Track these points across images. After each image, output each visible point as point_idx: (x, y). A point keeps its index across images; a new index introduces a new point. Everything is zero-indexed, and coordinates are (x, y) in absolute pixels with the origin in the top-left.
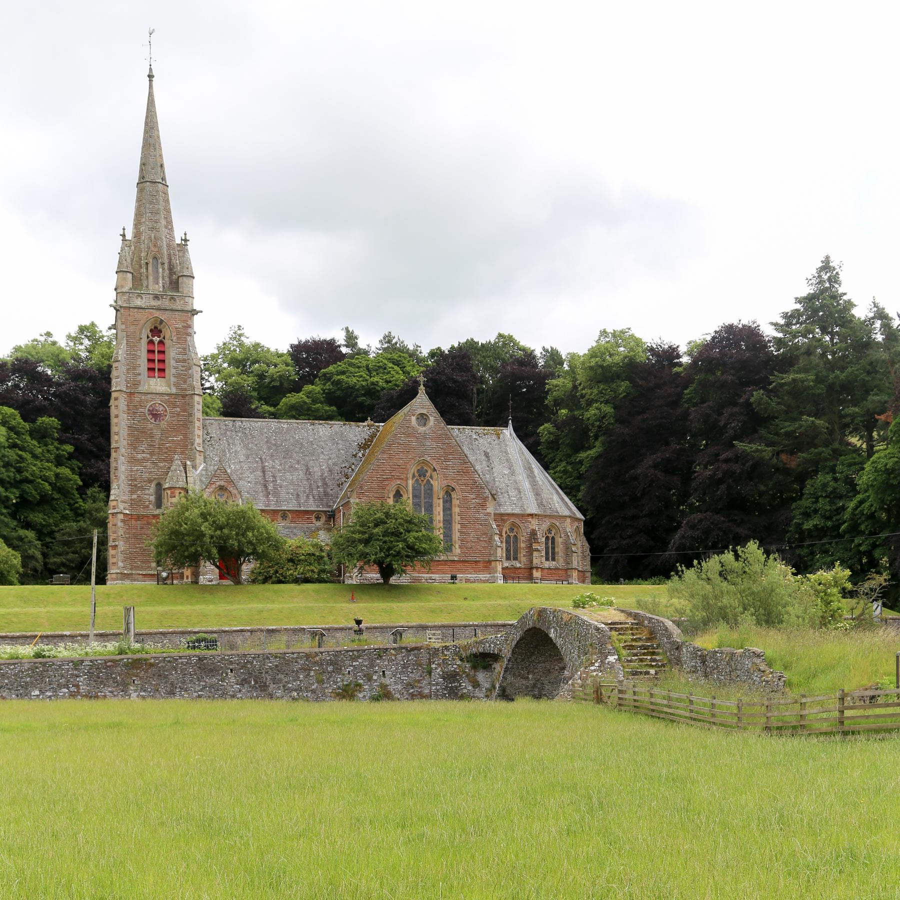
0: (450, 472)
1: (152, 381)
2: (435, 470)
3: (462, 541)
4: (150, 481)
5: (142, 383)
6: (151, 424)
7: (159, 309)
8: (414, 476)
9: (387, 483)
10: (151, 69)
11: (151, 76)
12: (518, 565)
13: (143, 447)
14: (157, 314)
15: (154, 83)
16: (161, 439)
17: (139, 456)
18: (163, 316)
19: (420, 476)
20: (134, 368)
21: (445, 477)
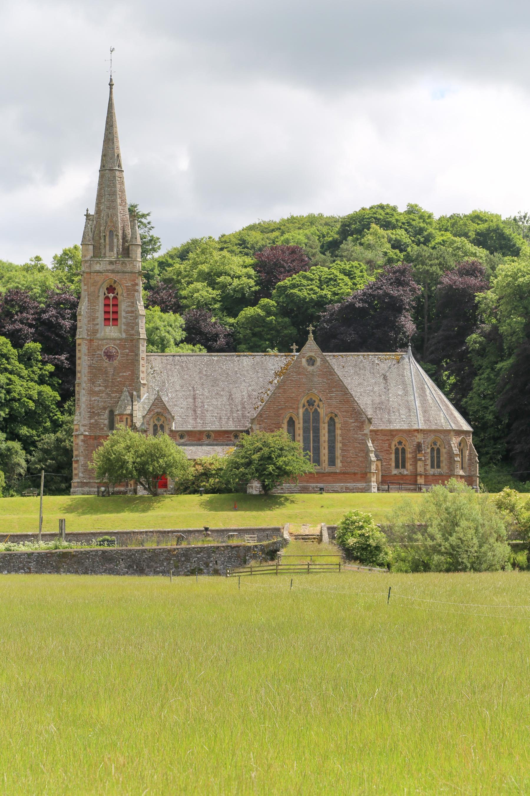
0: (334, 402)
1: (108, 329)
2: (321, 400)
3: (343, 457)
4: (105, 408)
5: (99, 331)
6: (106, 363)
7: (113, 272)
8: (304, 406)
9: (281, 412)
10: (111, 79)
11: (111, 85)
12: (406, 473)
13: (100, 382)
14: (111, 276)
15: (113, 90)
16: (113, 375)
17: (97, 389)
18: (117, 277)
19: (309, 405)
20: (94, 320)
21: (329, 405)
